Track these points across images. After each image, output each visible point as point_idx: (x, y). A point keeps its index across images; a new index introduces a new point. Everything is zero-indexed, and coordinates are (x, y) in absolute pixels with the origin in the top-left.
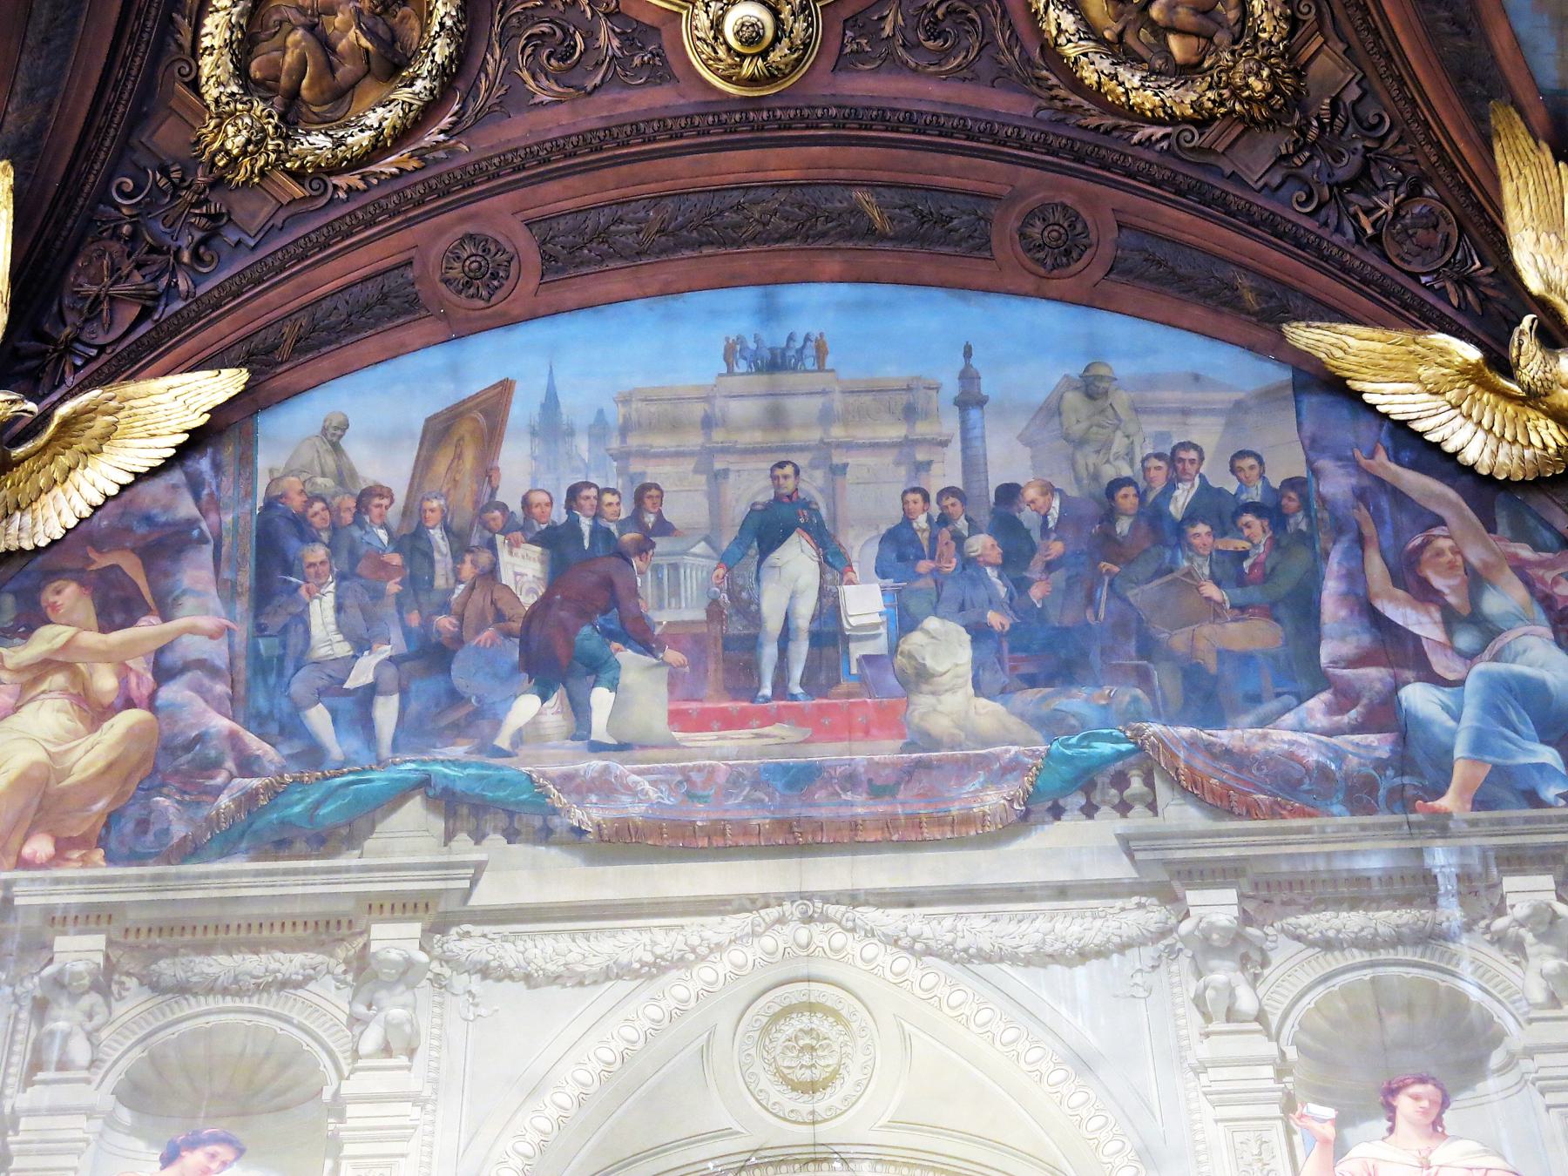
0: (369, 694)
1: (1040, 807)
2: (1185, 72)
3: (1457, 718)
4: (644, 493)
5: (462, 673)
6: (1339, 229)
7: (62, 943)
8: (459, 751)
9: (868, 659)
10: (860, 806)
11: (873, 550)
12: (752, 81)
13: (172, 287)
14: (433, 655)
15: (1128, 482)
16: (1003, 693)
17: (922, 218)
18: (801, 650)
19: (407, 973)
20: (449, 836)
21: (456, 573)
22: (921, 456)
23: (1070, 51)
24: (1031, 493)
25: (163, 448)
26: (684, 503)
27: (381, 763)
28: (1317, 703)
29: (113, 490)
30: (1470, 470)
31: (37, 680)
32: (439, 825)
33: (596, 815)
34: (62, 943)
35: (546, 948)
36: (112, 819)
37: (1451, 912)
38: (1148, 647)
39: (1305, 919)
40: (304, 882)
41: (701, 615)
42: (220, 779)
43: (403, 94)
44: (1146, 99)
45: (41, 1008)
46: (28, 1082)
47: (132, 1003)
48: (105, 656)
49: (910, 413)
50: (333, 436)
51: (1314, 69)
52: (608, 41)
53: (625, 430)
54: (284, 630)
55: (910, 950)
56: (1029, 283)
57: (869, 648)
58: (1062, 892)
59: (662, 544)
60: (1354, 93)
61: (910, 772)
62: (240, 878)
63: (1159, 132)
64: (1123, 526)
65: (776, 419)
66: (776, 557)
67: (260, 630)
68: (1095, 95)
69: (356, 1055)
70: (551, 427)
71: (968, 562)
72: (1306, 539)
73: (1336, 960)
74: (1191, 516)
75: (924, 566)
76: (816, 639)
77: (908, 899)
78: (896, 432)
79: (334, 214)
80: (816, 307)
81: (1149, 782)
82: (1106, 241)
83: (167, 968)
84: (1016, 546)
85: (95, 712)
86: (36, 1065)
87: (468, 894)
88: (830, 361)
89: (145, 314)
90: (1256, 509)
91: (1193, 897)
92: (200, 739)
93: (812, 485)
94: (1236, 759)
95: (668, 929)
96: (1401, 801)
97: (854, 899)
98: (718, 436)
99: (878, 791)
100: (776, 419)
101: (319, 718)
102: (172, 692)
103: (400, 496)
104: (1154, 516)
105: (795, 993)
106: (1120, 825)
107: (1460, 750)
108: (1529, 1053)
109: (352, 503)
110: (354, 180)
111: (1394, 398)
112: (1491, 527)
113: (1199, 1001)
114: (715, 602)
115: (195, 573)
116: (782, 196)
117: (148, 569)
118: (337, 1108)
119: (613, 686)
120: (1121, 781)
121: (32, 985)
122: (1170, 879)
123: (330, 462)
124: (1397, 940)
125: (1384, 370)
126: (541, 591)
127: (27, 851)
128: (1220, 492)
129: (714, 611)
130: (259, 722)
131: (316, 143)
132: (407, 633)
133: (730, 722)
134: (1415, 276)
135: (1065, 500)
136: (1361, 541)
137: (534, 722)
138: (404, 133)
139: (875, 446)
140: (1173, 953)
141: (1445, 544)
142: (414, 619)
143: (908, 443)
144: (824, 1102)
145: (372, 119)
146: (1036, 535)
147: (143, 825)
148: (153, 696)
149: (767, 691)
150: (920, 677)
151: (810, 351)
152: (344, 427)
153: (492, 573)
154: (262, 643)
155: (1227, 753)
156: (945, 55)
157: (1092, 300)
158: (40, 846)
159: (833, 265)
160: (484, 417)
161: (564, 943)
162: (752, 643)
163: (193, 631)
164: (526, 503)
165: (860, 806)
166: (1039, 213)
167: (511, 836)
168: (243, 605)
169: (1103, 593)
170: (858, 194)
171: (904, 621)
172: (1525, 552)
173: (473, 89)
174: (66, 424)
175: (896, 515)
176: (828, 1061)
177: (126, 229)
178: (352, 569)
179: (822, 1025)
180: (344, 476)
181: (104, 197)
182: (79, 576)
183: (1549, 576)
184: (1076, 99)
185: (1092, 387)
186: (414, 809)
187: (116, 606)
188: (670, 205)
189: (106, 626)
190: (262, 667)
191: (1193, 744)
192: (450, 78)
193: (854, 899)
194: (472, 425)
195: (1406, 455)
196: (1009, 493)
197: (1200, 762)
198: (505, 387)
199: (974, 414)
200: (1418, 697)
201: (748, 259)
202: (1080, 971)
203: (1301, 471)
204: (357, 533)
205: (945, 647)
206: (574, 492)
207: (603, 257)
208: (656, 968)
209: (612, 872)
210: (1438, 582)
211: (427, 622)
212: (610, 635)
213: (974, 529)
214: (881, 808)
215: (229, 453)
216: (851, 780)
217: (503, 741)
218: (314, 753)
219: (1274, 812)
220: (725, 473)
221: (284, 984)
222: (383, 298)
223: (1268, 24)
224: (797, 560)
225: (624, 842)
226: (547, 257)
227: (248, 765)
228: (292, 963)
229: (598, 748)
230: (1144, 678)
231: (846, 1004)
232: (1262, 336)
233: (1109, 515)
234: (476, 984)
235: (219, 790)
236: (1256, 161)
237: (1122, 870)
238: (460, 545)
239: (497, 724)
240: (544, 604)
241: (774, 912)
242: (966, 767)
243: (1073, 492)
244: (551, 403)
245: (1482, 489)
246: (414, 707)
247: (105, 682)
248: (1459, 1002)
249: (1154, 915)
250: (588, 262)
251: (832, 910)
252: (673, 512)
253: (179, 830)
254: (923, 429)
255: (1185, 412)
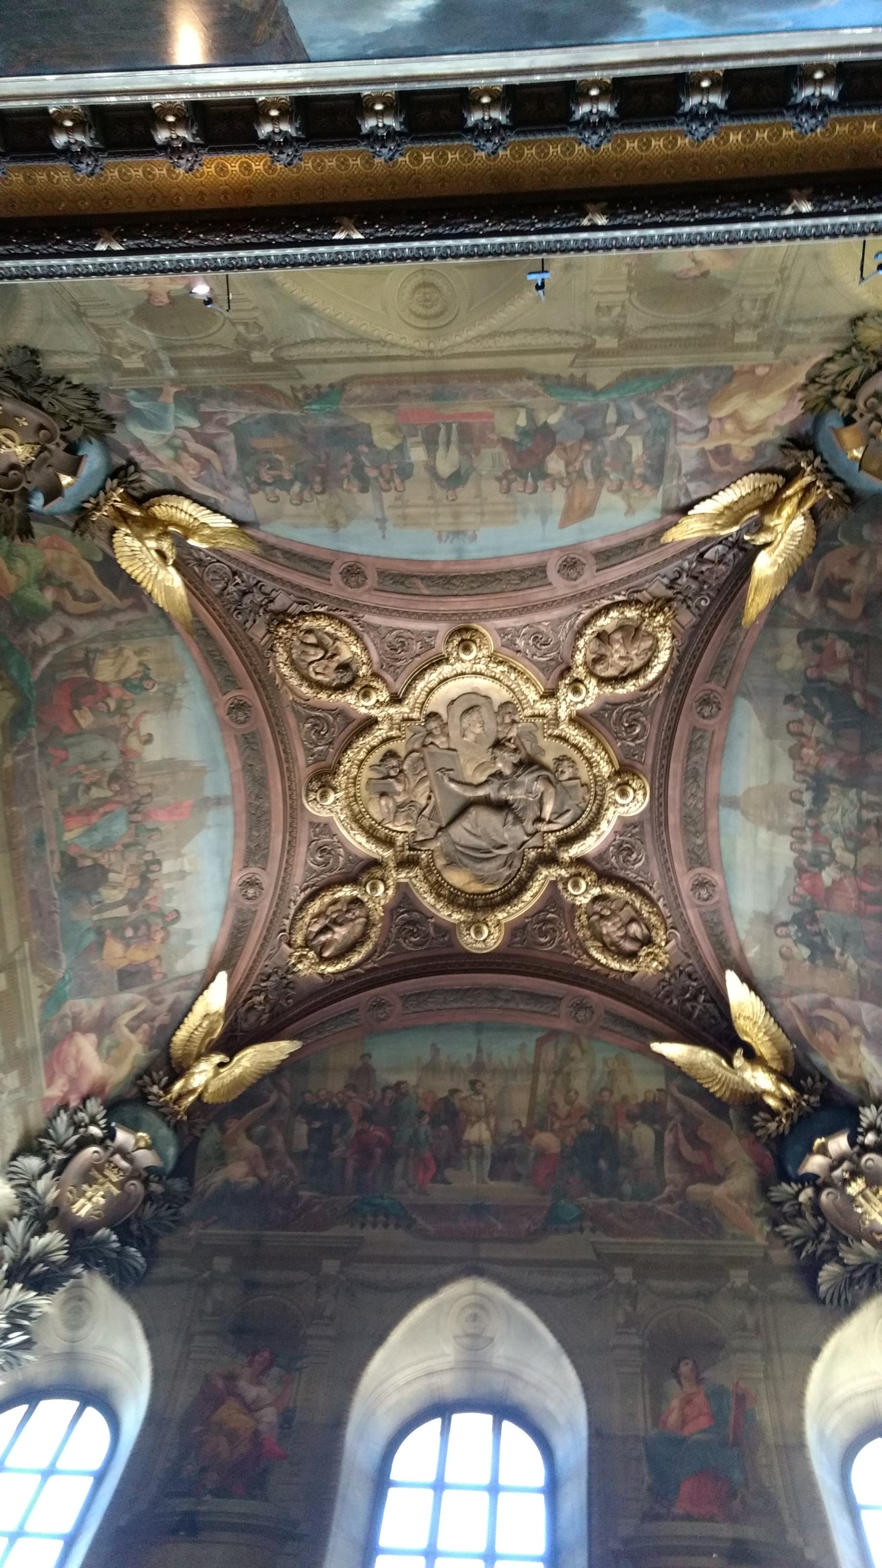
0: (618, 423)
1: (339, 389)
2: (309, 631)
3: (176, 417)
4: (508, 491)
5: (581, 431)
6: (249, 577)
7: (755, 339)
8: (580, 404)
9: (416, 435)
10: (413, 388)
11: (415, 471)
12: (467, 629)
13: (691, 563)
14: (591, 436)
15: (318, 493)
16: (359, 425)
17: (402, 583)
18: (442, 438)
19: (602, 332)
20: (585, 376)
21: (582, 464)
22: (399, 503)
23: (352, 638)
24: (355, 490)
25: (698, 509)
26: (491, 489)
27: (614, 400)
28: (231, 421)
29: (721, 493)
30: (188, 497)
31: (758, 427)
32: (589, 380)
33: (523, 384)
34: (755, 339)
35: (542, 340)
36: (729, 380)
37: (163, 356)
38: (303, 439)
39: (222, 353)
40: (646, 361)
41: (482, 450)
42: (682, 395)
43: (595, 629)
44: (323, 623)
45: (764, 318)
46: (770, 296)
47: (723, 319)
48: (728, 436)
49: (405, 517)
50: (630, 510)
51: (265, 632)
52: (521, 643)
53: (515, 512)
54: (653, 445)
55: (386, 342)
56: (362, 560)
57: (414, 439)
58: (325, 361)
59: (500, 474)
60: (248, 625)
61: (394, 399)
62: (674, 362)
63: (318, 609)
64: (318, 479)
65: (456, 515)
66: (454, 470)
67: (664, 445)
68: (342, 623)
69: (623, 306)
70: (544, 514)
71: (378, 468)
72: (246, 474)
73: (208, 341)
74: (291, 483)
75: (395, 466)
76: (436, 443)
77: (388, 358)
78: (410, 511)
79: (627, 586)
80: (440, 553)
81: (296, 397)
82: (335, 575)
83: (707, 332)
84: (358, 472)
85: (734, 416)
86: (767, 301)
87: (576, 358)
88: (436, 534)
89: (702, 555)
90: (266, 484)
91: (271, 360)
92: (690, 408)
93: (441, 493)
94: (260, 403)
95: (490, 347)
96: (192, 390)
97: (411, 358)
98: (478, 510)
99: (407, 392)
100: (456, 515)
101: (640, 415)
102: (702, 423)
103: (604, 491)
104: (307, 482)
105: (434, 323)
106: (303, 382)
107: (172, 407)
108: (116, 315)
109: (624, 488)
110: (618, 598)
111: (221, 522)
112: (175, 478)
113: (261, 328)
114: (477, 455)
115: (689, 463)
116: (455, 592)
117: (709, 465)
118: (630, 290)
119: (517, 427)
120: (307, 397)
121: (767, 326)
122: (279, 365)
123: (632, 501)
124: (182, 347)
125: (225, 532)
126: (548, 458)
127: (767, 370)
128: (281, 489)
129: (477, 452)
130: (665, 413)
131: (632, 613)
132: (602, 444)
133: (470, 415)
134: (218, 561)
135: (341, 487)
136: (225, 473)
137: (549, 415)
138: (597, 615)
139: (416, 506)
140: (275, 342)
141: (192, 472)
142: (599, 448)
143: (405, 506)
144: (419, 278)
145: (608, 620)
146: (352, 476)
147: (716, 379)
148: (709, 422)
149: (454, 426)
150: (392, 430)
151: (444, 538)
152: (627, 513)
153: (568, 464)
154: (663, 440)
155: (265, 405)
156: (398, 637)
157: (337, 553)
158: (761, 371)
159: (436, 567)
160: (570, 515)
161: (534, 342)
162: (461, 442)
163: (691, 444)
164: (554, 488)
165: (413, 388)
166: (359, 586)
167: (558, 377)
168: (670, 452)
169: (323, 457)
170: (426, 592)
171: (401, 449)
172: (161, 470)
173: (571, 627)
174: (736, 523)
175: (407, 483)
176: (419, 296)
177: (706, 587)
178: (625, 466)
179: (421, 310)
180: (627, 497)
181: (713, 600)
182: (737, 462)
183: (150, 462)
184: (350, 620)
185: (335, 525)
186: (600, 385)
187: (723, 453)
188: (498, 589)
189: (728, 448)
190: (664, 432)
191: (280, 408)
192: (579, 634)
193: (411, 358)
194: (575, 513)
195: (212, 501)
196: (364, 490)
197: (276, 402)
198: (562, 525)
199: (380, 516)
200: (194, 424)
201: (467, 569)
202: (313, 336)
203: (252, 496)
204: (622, 478)
205: (384, 440)
206: (535, 490)
207: (522, 571)
208: (493, 335)
209: (515, 366)
210: (192, 460)
211: (594, 447)
212: (519, 443)
213: (376, 479)
214: (403, 387)
215: (673, 505)
216: (417, 396)
217: (562, 409)
218: (642, 403)
219: (243, 387)
220: (476, 497)
221: (655, 328)
222: (608, 558)
223: (280, 650)
224: (445, 468)
225: (511, 375)
226: (544, 571)
227: (671, 399)
228: (650, 335)
229: (522, 406)
230: (303, 429)
231: (412, 320)
232: (272, 540)
233: (323, 483)
234: (571, 329)
235: (684, 390)
236: (281, 601)
237: (301, 368)
238: (581, 474)
239: (565, 414)
240: (548, 452)
241: (445, 353)
242: (370, 400)
243: (339, 491)
244: (544, 522)
245: (180, 492)
246: (600, 419)
247: (729, 427)
248: (151, 328)
249: (285, 354)
250: (529, 569)
251: (421, 354)
252: (495, 484)
253: (701, 377)
254: (399, 512)
255: (299, 516)
